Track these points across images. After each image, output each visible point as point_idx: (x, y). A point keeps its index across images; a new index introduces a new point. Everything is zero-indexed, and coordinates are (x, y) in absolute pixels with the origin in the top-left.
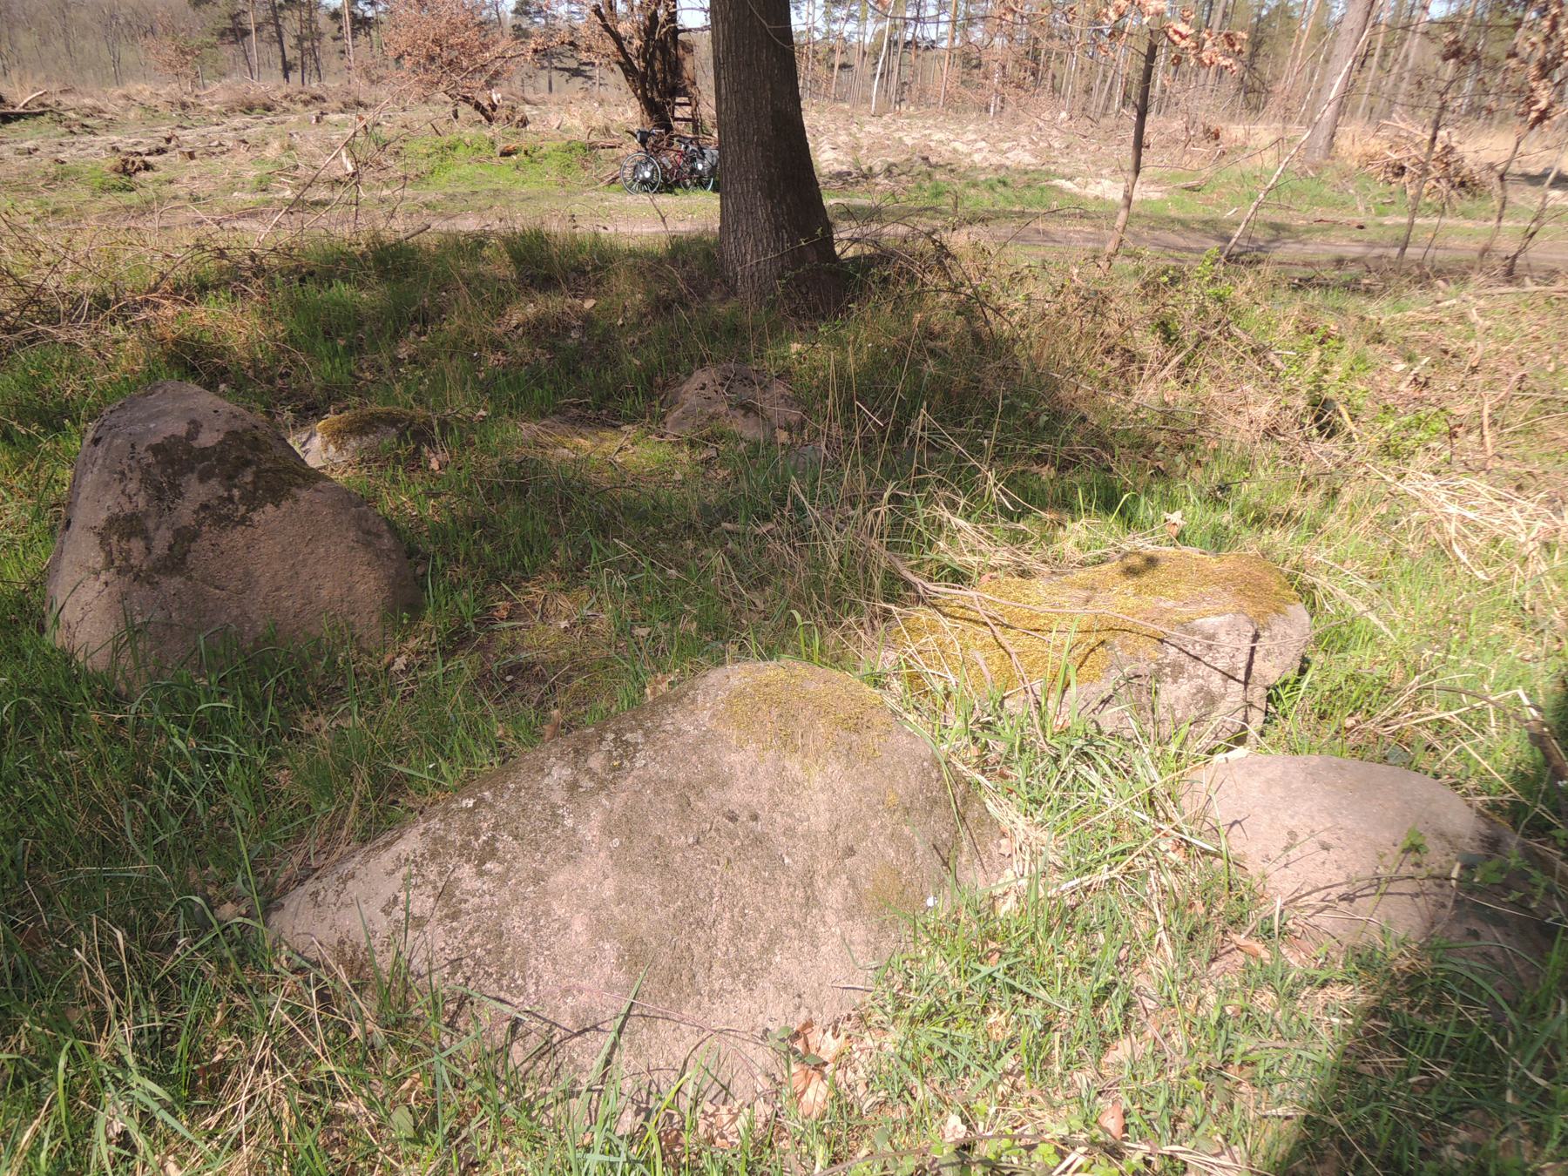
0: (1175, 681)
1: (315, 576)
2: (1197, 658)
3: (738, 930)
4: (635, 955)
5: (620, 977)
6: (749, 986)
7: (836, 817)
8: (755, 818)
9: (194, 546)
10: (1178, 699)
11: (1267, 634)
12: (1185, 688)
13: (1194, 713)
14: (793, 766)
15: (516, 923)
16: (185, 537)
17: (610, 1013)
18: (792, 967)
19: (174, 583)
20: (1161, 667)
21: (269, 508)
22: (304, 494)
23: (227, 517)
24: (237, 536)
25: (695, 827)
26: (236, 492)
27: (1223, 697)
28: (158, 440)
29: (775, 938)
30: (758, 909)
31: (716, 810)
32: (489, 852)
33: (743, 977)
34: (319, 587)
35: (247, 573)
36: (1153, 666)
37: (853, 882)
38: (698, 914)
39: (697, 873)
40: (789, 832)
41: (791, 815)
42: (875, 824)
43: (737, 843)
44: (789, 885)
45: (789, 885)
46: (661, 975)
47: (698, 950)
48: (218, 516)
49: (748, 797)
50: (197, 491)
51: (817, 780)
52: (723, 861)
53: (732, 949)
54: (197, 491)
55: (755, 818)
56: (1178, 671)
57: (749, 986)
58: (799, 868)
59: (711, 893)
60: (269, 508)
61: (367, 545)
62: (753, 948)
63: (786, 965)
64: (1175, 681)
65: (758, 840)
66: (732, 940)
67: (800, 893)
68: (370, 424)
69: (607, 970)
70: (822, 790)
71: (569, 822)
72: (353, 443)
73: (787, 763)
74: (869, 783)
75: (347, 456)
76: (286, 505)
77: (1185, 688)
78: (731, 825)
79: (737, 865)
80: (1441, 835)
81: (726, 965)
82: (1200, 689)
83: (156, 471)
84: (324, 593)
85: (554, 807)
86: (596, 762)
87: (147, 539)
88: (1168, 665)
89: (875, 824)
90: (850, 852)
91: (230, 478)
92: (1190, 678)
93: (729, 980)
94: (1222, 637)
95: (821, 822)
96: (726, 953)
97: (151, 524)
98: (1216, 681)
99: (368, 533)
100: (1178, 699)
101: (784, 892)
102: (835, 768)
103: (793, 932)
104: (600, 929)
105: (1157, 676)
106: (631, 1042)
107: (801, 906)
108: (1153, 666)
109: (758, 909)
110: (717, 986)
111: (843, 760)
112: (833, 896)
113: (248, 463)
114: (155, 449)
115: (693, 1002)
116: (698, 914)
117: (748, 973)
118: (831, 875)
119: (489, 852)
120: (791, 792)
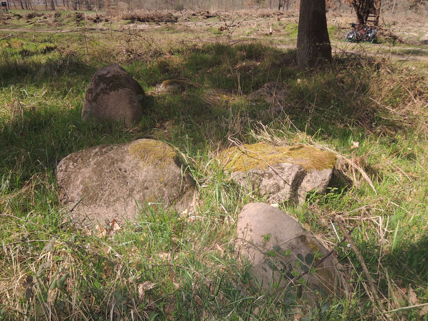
0: (269, 179)
1: (119, 108)
2: (277, 174)
3: (110, 194)
4: (86, 190)
5: (80, 193)
6: (107, 207)
7: (146, 179)
8: (125, 171)
9: (99, 97)
10: (268, 184)
11: (309, 174)
12: (271, 182)
13: (272, 190)
14: (141, 164)
15: (72, 176)
16: (98, 94)
17: (76, 200)
18: (119, 208)
19: (94, 104)
20: (265, 173)
21: (113, 92)
22: (120, 90)
23: (105, 92)
24: (106, 97)
25: (111, 169)
26: (108, 87)
27: (283, 188)
28: (100, 74)
29: (118, 199)
30: (117, 192)
31: (118, 167)
32: (76, 161)
33: (107, 205)
34: (119, 111)
35: (107, 105)
36: (263, 172)
37: (144, 195)
38: (102, 187)
39: (106, 178)
40: (132, 178)
41: (135, 174)
42: (155, 184)
43: (119, 176)
44: (126, 189)
45: (126, 189)
46: (90, 197)
47: (100, 195)
48: (104, 91)
49: (126, 167)
50: (102, 86)
51: (145, 169)
52: (113, 178)
53: (107, 198)
54: (102, 86)
55: (125, 171)
56: (270, 176)
57: (107, 207)
58: (130, 187)
59: (107, 184)
60: (113, 92)
61: (130, 104)
62: (112, 199)
63: (118, 207)
64: (269, 179)
65: (124, 177)
66: (108, 196)
67: (128, 192)
68: (173, 83)
69: (79, 191)
70: (145, 172)
71: (90, 160)
72: (168, 87)
73: (140, 163)
74: (158, 174)
75: (166, 90)
76: (116, 91)
77: (271, 182)
78: (119, 171)
79: (116, 180)
80: (276, 238)
81: (104, 200)
82: (276, 184)
83: (97, 81)
84: (120, 112)
85: (91, 156)
86: (104, 150)
87: (92, 94)
88: (268, 173)
89: (155, 184)
90: (147, 188)
91: (108, 84)
92: (274, 179)
93: (103, 204)
94: (286, 170)
95: (141, 179)
96: (106, 198)
97: (93, 91)
98: (281, 183)
99: (132, 101)
100: (268, 184)
101: (124, 190)
102: (151, 167)
103: (123, 200)
104: (82, 183)
105: (263, 175)
106: (78, 207)
107: (127, 195)
108: (263, 172)
109: (117, 192)
110: (100, 204)
111: (153, 166)
112: (137, 197)
113: (112, 81)
114: (99, 76)
115: (94, 205)
116: (102, 187)
117: (108, 204)
118: (139, 192)
119: (76, 161)
120: (137, 169)
